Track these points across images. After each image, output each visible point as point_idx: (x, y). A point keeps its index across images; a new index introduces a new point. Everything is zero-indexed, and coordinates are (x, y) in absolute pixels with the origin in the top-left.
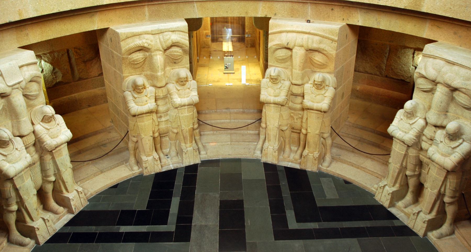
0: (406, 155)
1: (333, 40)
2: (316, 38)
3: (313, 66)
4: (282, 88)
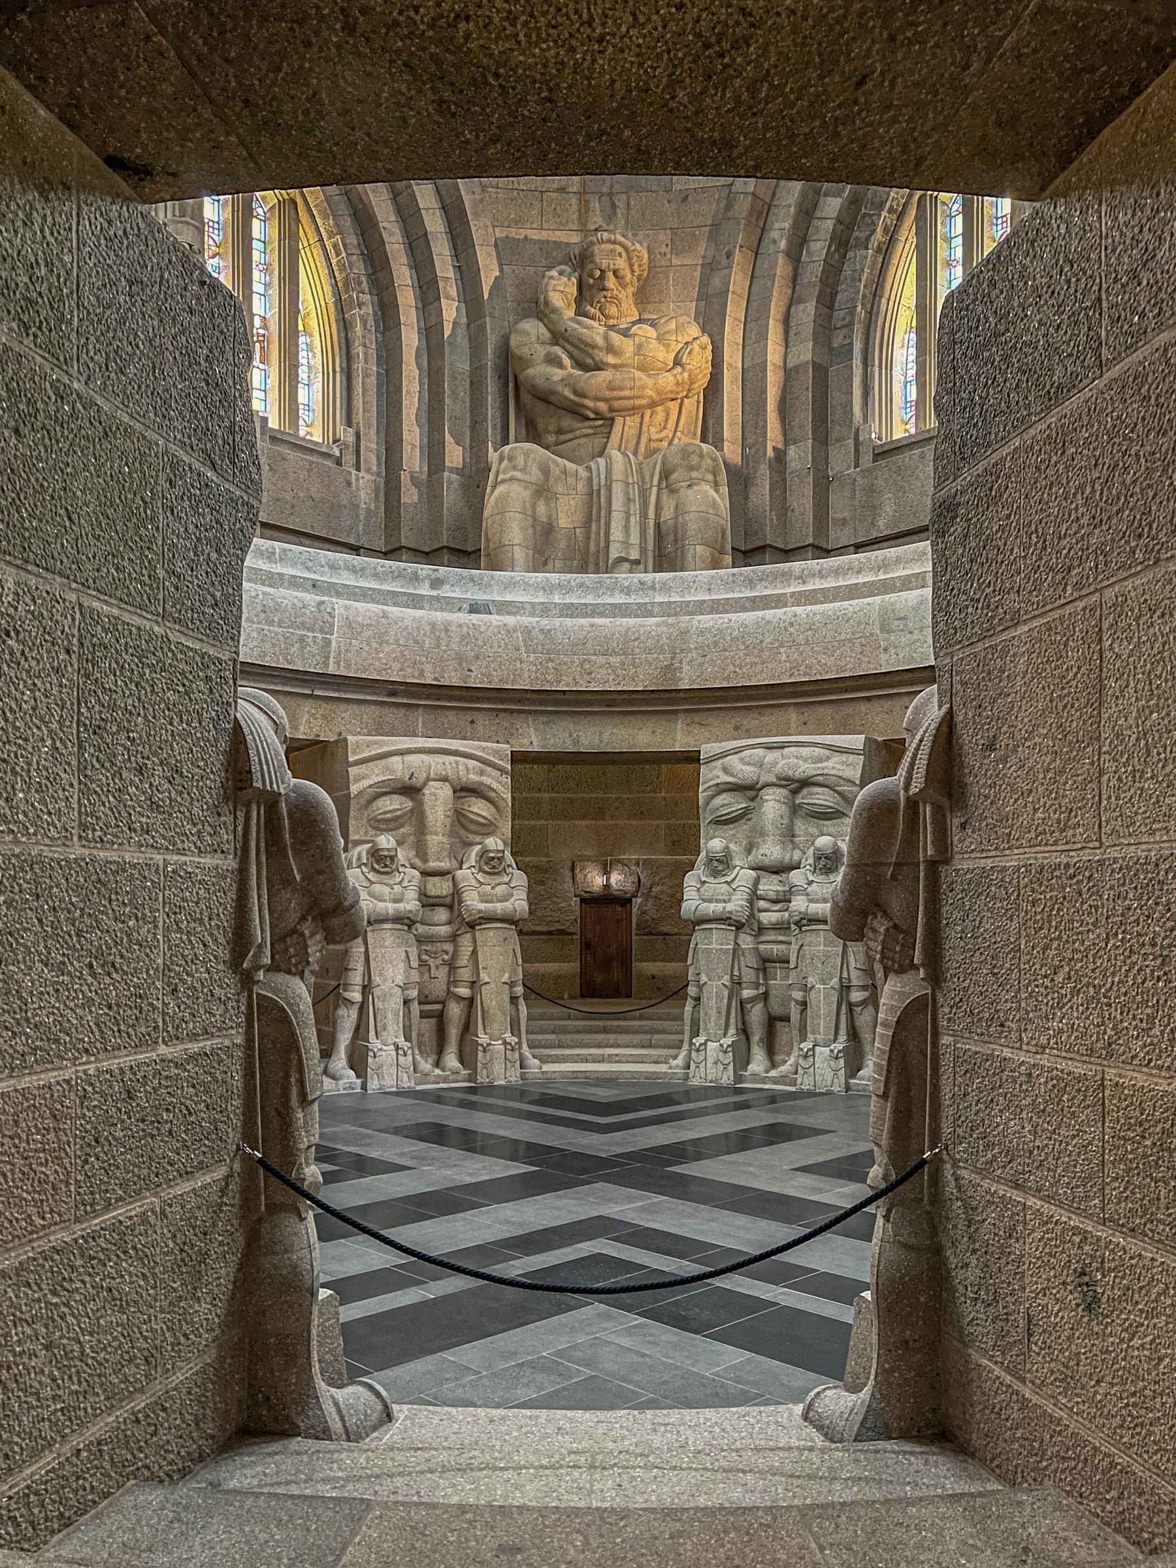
0: (736, 951)
1: (502, 770)
2: (472, 763)
3: (466, 829)
4: (405, 884)
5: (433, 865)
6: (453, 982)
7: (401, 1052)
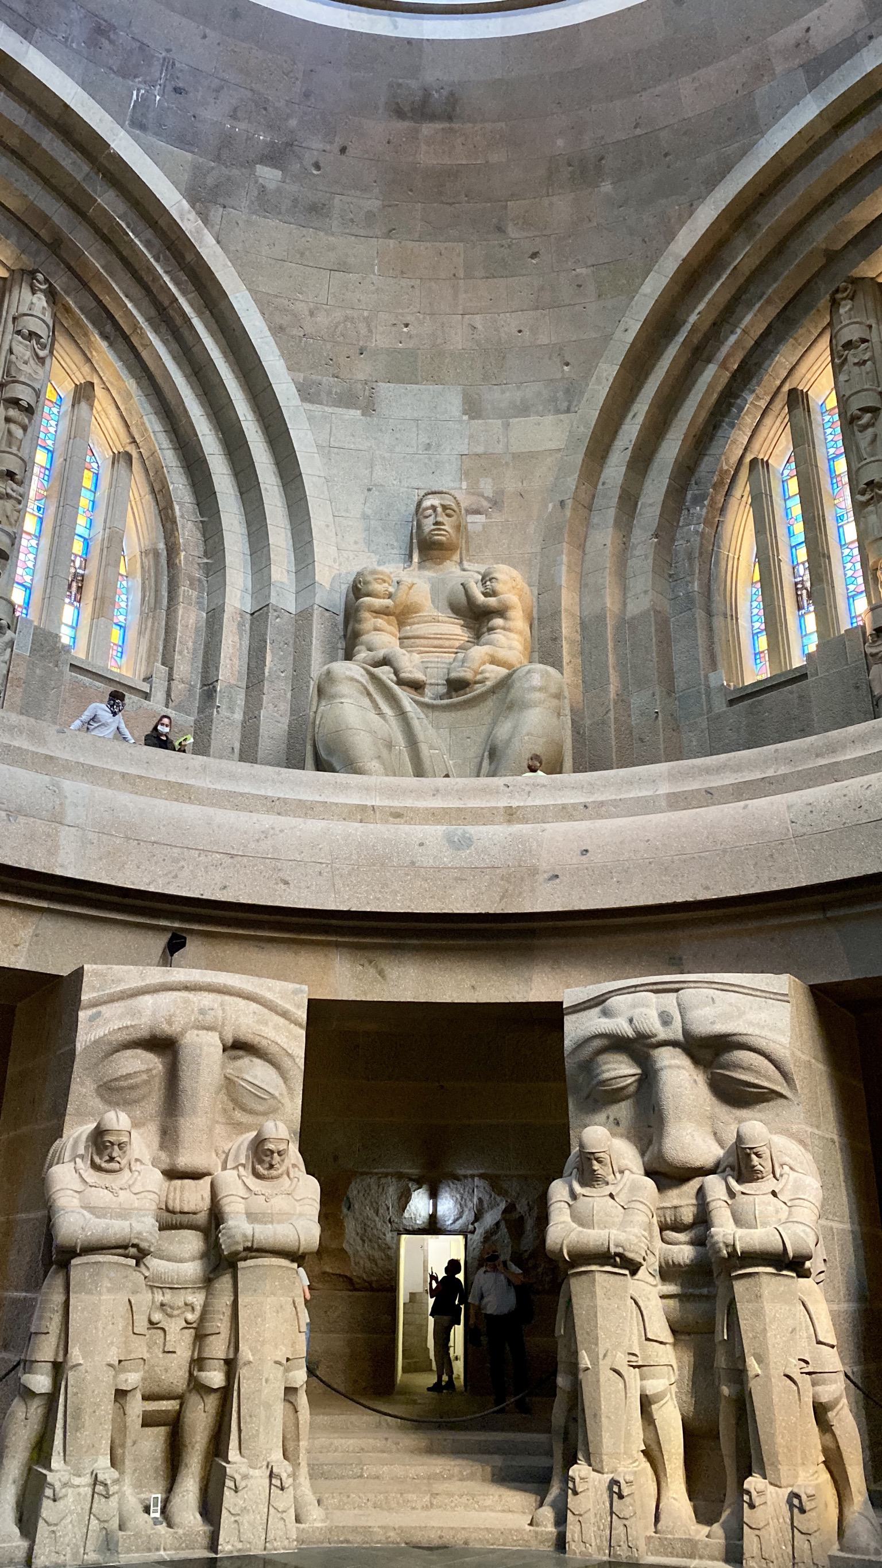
5: (185, 1160)
6: (198, 1362)
7: (99, 1488)
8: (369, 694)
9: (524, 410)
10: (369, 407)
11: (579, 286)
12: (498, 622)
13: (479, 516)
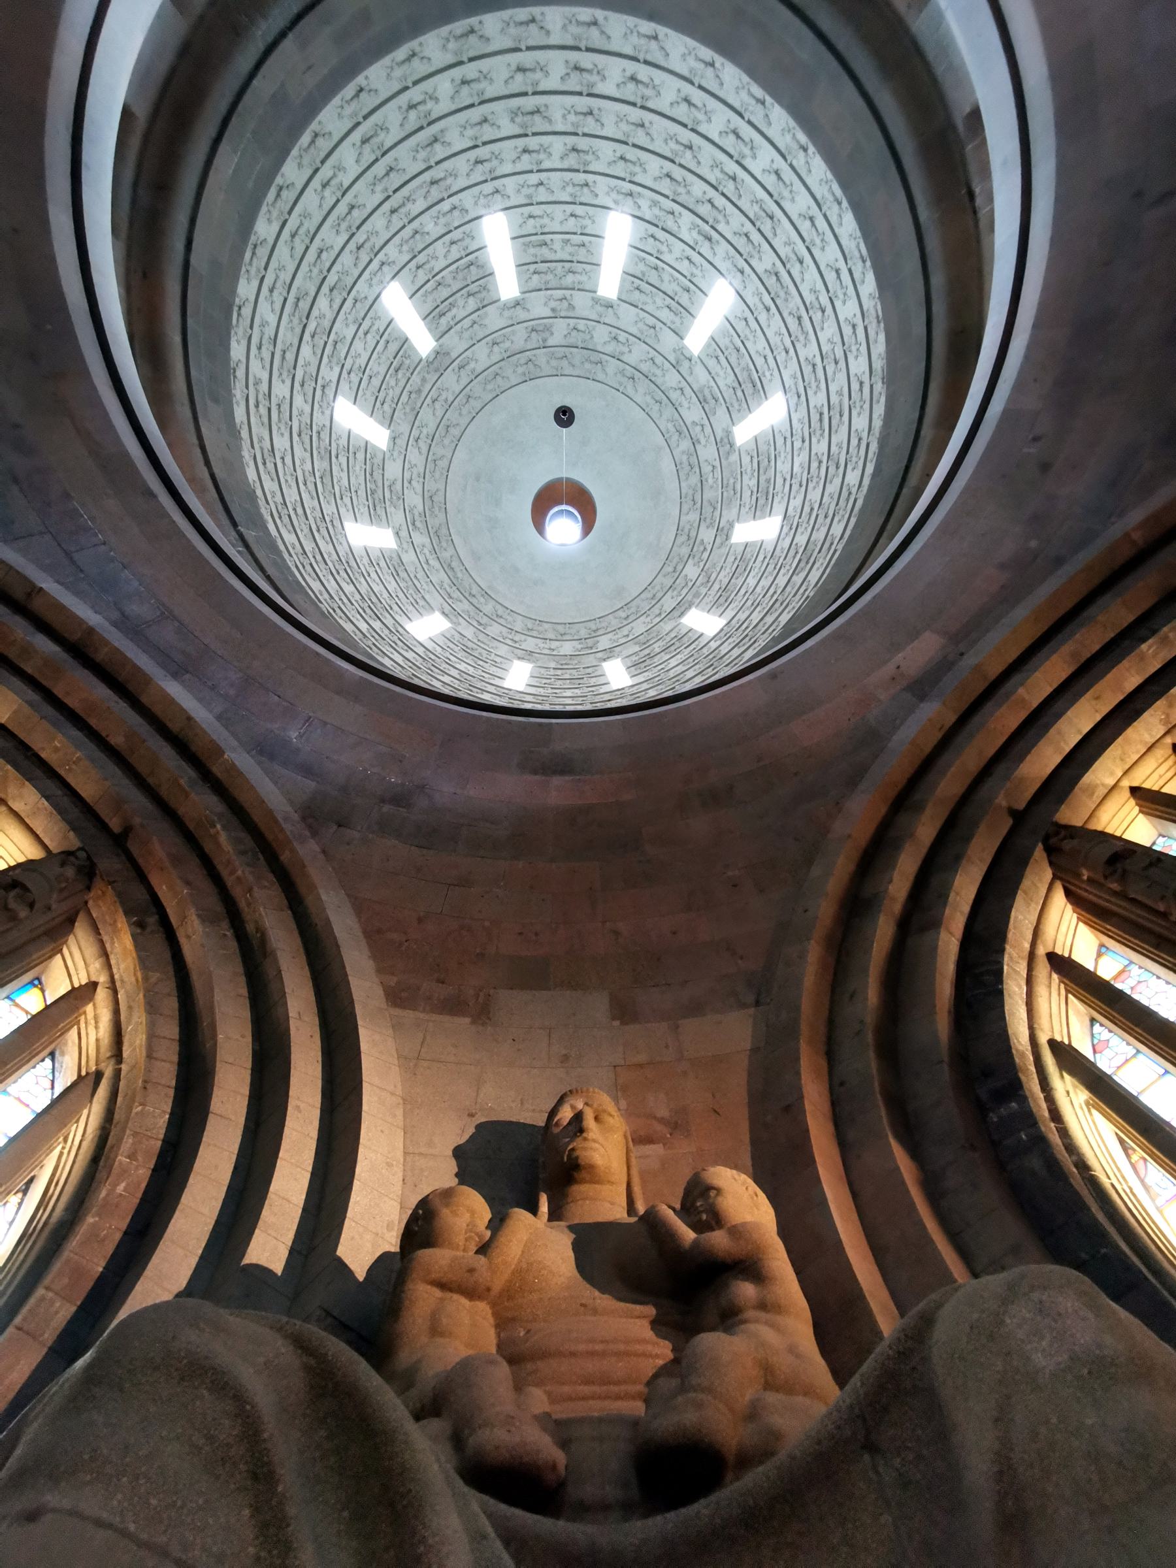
8: (262, 1475)
9: (695, 1009)
10: (483, 1014)
11: (735, 886)
12: (746, 1290)
13: (652, 1146)
